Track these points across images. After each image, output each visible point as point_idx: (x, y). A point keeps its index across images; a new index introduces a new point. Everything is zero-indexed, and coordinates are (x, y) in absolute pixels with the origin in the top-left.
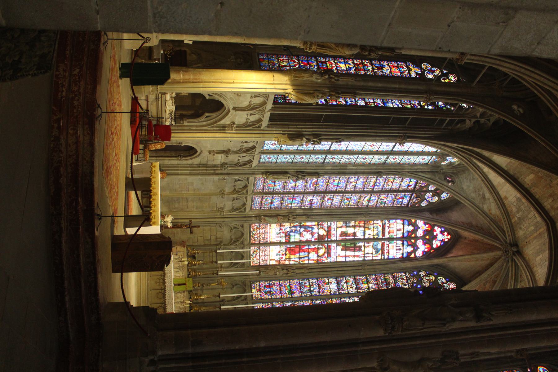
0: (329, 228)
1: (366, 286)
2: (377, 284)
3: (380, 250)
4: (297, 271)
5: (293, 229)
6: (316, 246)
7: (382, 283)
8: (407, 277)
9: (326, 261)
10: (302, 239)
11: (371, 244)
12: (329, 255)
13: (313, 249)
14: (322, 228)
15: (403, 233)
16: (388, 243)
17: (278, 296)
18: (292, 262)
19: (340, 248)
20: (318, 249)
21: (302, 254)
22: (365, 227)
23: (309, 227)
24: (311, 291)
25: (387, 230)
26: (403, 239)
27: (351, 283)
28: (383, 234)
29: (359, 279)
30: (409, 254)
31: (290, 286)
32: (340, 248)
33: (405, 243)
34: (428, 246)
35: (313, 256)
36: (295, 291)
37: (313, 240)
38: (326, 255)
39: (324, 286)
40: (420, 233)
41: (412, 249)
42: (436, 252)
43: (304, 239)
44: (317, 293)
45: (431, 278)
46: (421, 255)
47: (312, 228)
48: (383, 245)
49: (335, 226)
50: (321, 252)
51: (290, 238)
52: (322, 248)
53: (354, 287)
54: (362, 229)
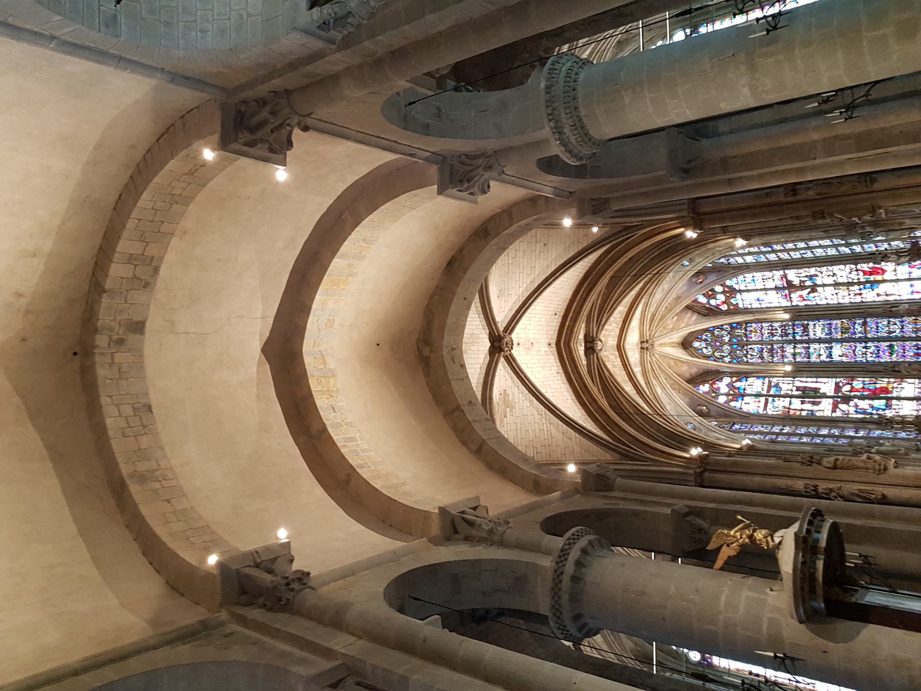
0: (834, 411)
1: (797, 351)
2: (783, 351)
3: (774, 386)
4: (881, 368)
5: (881, 412)
6: (852, 394)
7: (777, 352)
8: (746, 357)
9: (842, 379)
10: (871, 402)
11: (782, 393)
12: (837, 384)
13: (857, 391)
14: (843, 411)
15: (743, 400)
16: (763, 392)
17: (908, 343)
18: (886, 380)
19: (821, 391)
20: (850, 391)
21: (872, 387)
22: (789, 408)
23: (861, 413)
24: (866, 347)
25: (762, 404)
26: (743, 396)
27: (815, 354)
28: (767, 401)
29: (803, 358)
30: (740, 380)
31: (891, 354)
32: (821, 391)
33: (742, 391)
34: (715, 386)
35: (858, 384)
36: (886, 348)
37: (856, 400)
38: (841, 384)
39: (849, 352)
40: (722, 399)
41: (734, 384)
42: (707, 380)
43: (867, 401)
44: (858, 345)
45: (720, 354)
46: (724, 378)
47: (856, 411)
48: (769, 391)
49: (826, 410)
50: (848, 388)
51: (887, 403)
52: (846, 391)
53: (811, 350)
54: (791, 407)
